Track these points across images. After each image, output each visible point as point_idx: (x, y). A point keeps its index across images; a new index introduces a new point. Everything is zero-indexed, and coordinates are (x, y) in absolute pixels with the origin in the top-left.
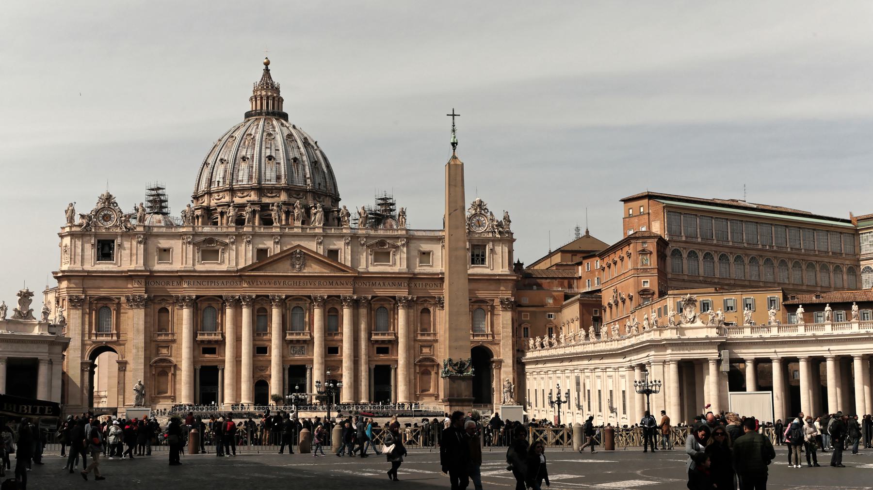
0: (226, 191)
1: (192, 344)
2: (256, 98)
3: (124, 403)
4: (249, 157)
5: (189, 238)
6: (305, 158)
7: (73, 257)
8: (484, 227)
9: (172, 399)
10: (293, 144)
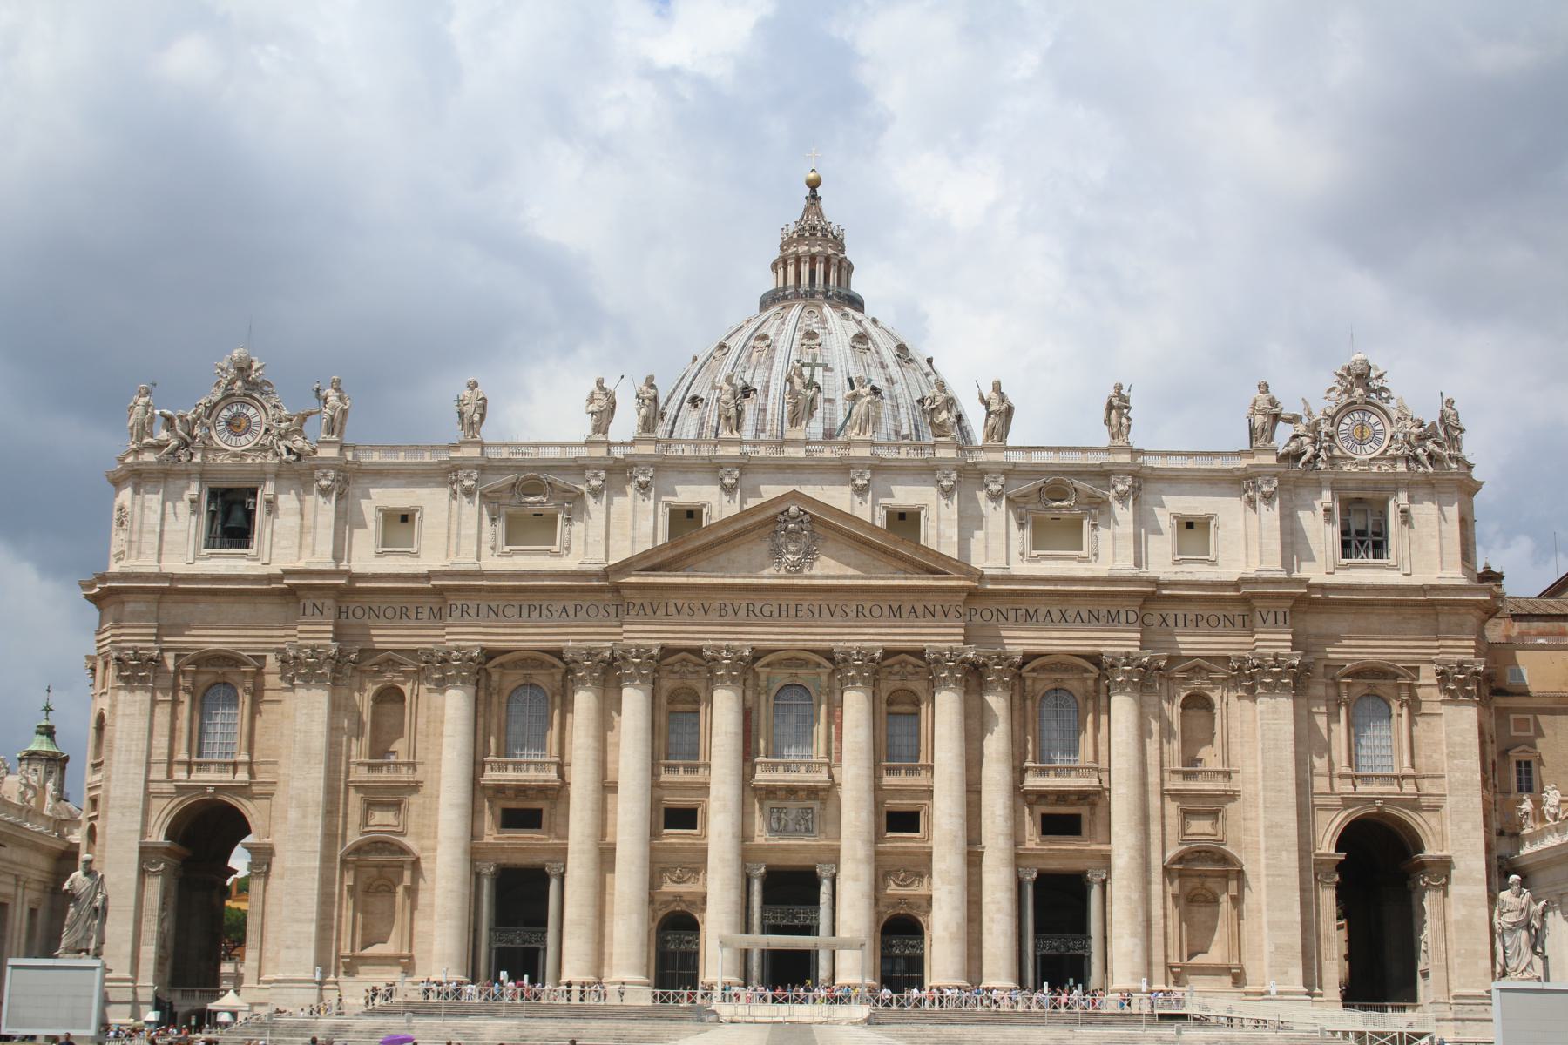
3: (259, 976)
8: (1380, 443)
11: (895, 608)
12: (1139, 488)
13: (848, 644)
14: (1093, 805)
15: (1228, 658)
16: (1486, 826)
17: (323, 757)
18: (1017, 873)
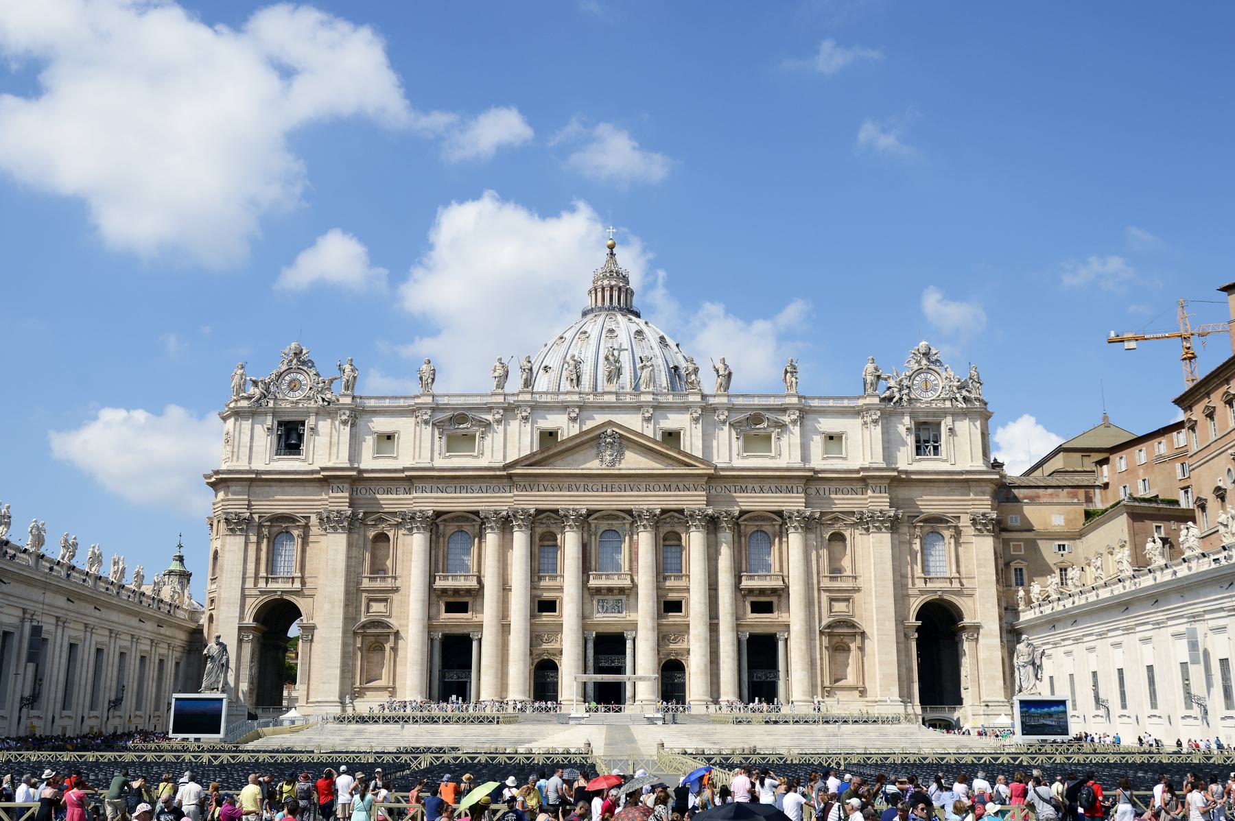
1: (427, 595)
2: (596, 290)
3: (308, 699)
7: (236, 450)
8: (935, 390)
9: (390, 692)
11: (667, 486)
12: (803, 417)
13: (641, 507)
14: (780, 596)
15: (854, 512)
16: (999, 605)
17: (343, 573)
18: (738, 635)
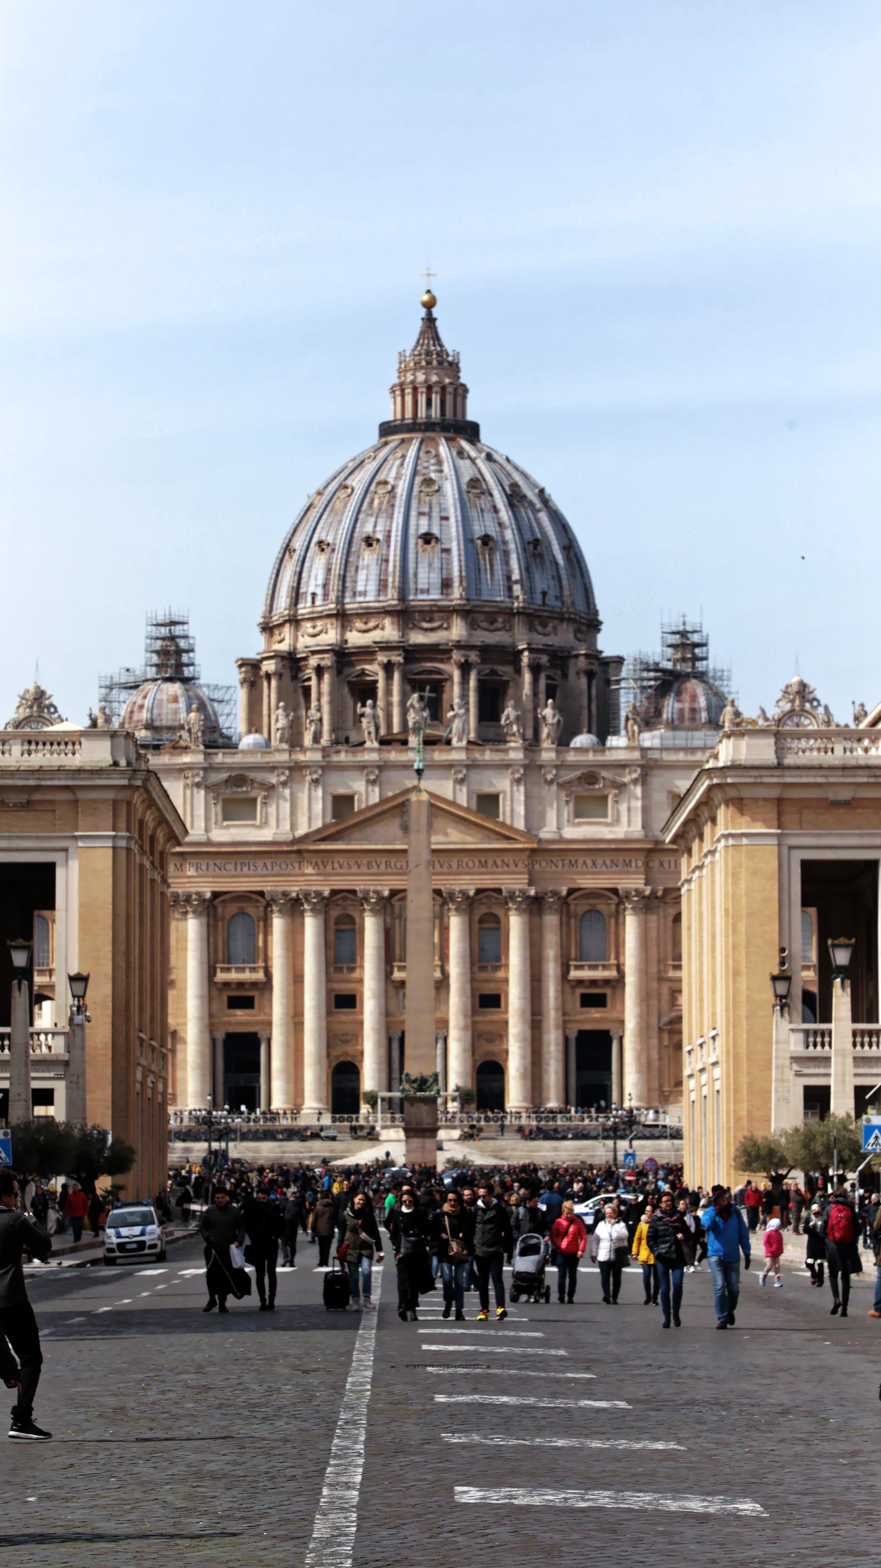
0: (329, 616)
2: (403, 390)
4: (380, 536)
5: (198, 775)
6: (509, 535)
10: (484, 502)
